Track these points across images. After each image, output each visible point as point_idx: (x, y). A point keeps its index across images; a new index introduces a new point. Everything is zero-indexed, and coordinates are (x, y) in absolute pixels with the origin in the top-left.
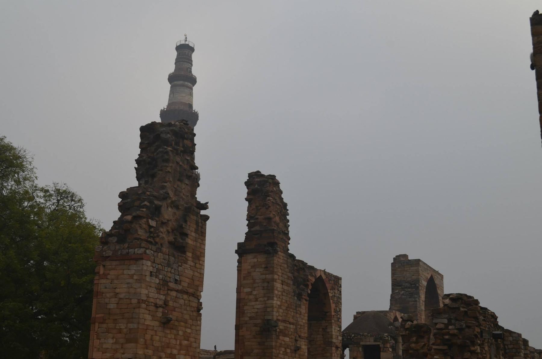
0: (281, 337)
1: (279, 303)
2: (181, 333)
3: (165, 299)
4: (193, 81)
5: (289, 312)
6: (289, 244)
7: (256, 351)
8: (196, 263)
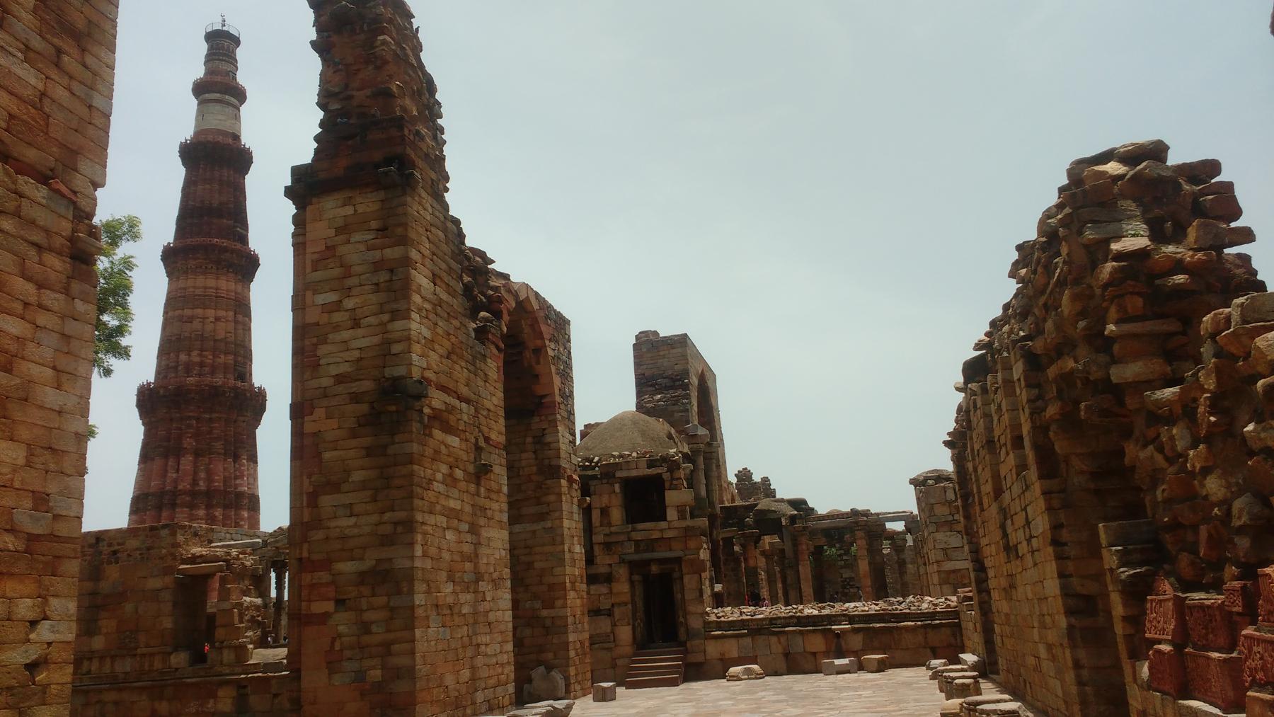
1: (427, 333)
4: (240, 95)
5: (457, 367)
6: (447, 190)
7: (357, 476)
8: (59, 51)
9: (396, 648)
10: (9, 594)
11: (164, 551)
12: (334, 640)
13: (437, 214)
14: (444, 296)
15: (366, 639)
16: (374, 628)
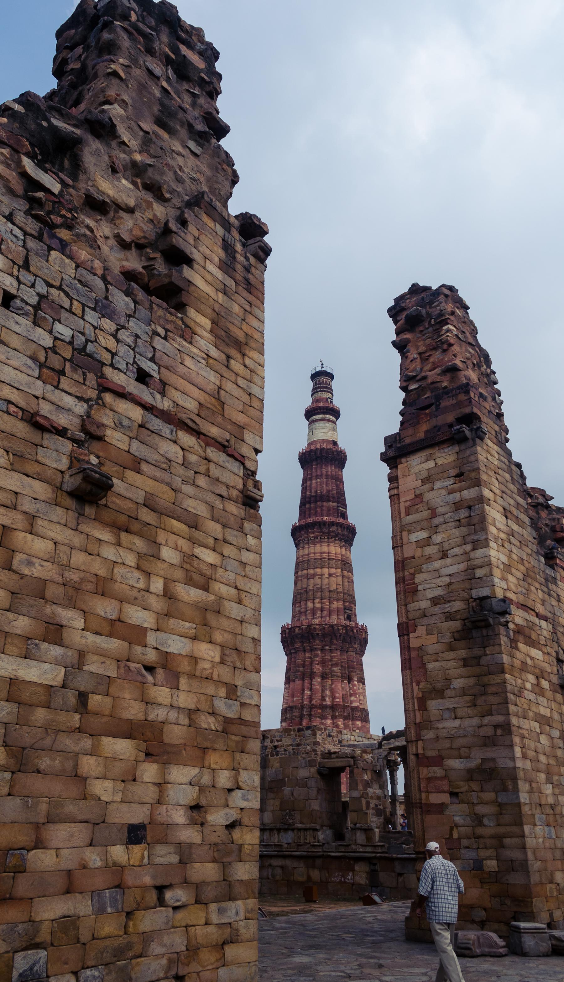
0: (521, 646)
1: (504, 559)
2: (168, 554)
3: (88, 415)
7: (458, 683)
9: (507, 841)
10: (213, 766)
11: (309, 747)
12: (451, 829)
13: (502, 458)
14: (515, 527)
15: (480, 831)
16: (486, 821)
